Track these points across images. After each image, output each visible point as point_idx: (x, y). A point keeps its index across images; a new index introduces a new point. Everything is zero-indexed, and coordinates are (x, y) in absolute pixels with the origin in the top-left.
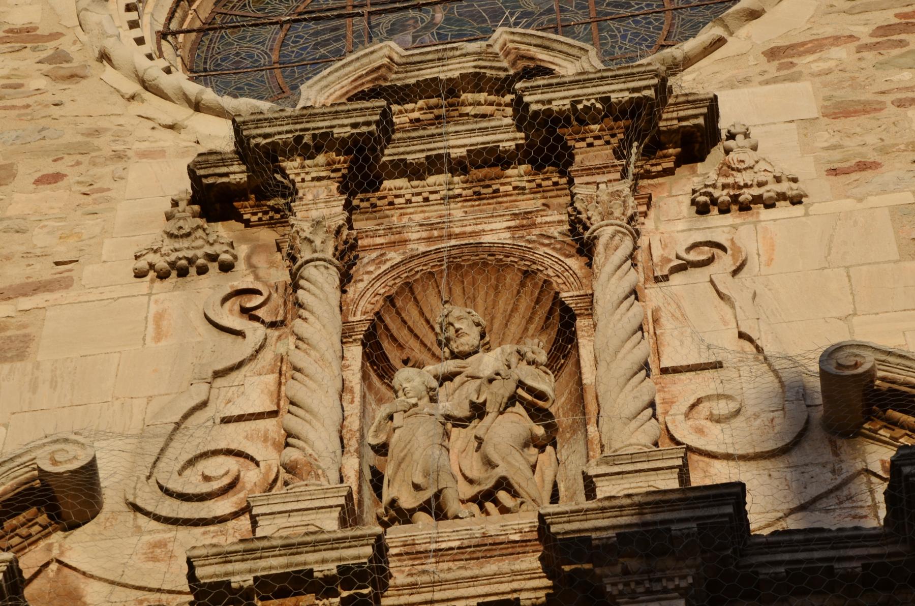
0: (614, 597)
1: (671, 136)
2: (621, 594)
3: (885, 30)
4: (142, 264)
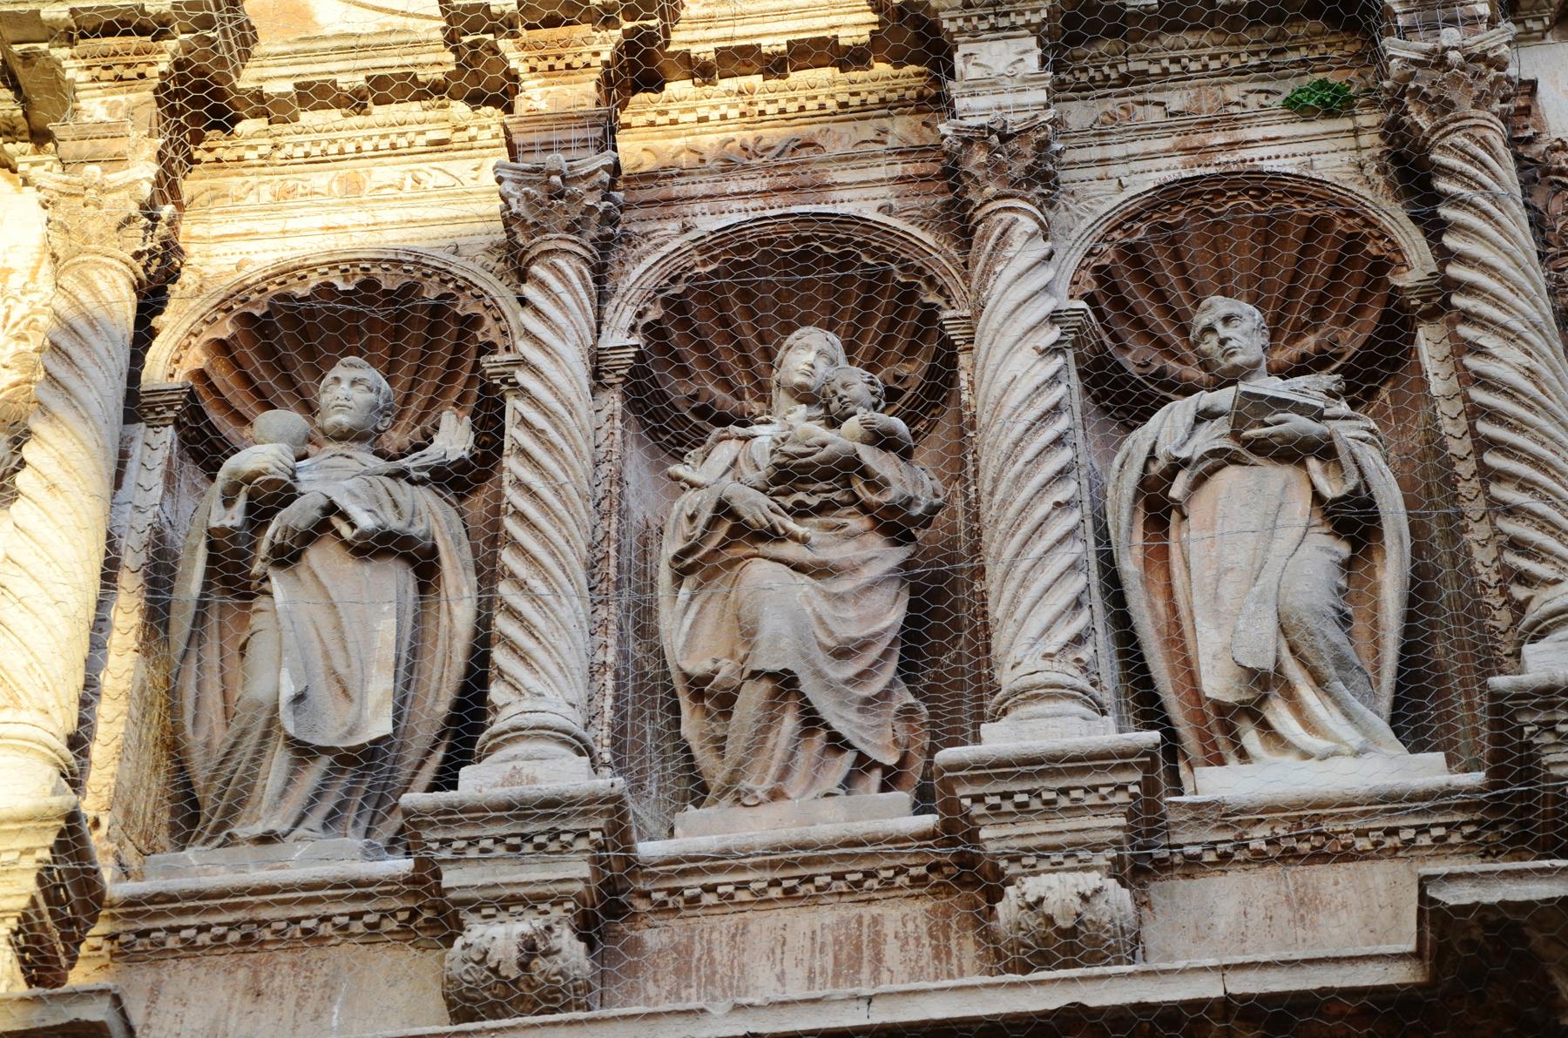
0: (951, 35)
2: (961, 31)
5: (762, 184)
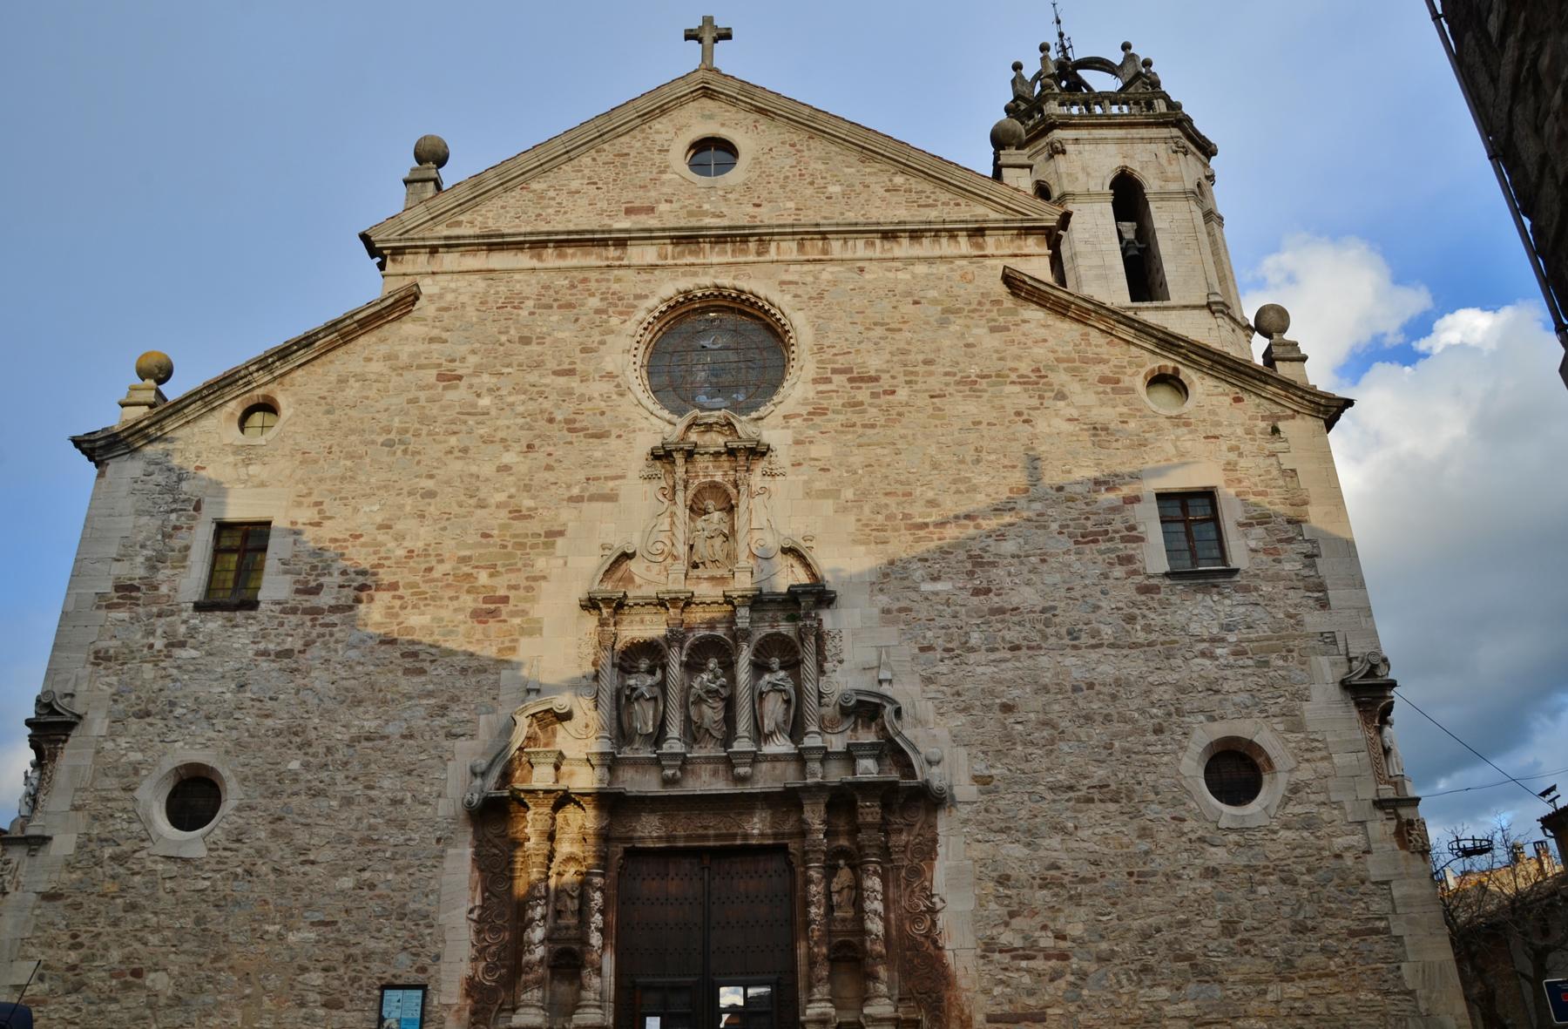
1: (758, 452)
3: (809, 413)
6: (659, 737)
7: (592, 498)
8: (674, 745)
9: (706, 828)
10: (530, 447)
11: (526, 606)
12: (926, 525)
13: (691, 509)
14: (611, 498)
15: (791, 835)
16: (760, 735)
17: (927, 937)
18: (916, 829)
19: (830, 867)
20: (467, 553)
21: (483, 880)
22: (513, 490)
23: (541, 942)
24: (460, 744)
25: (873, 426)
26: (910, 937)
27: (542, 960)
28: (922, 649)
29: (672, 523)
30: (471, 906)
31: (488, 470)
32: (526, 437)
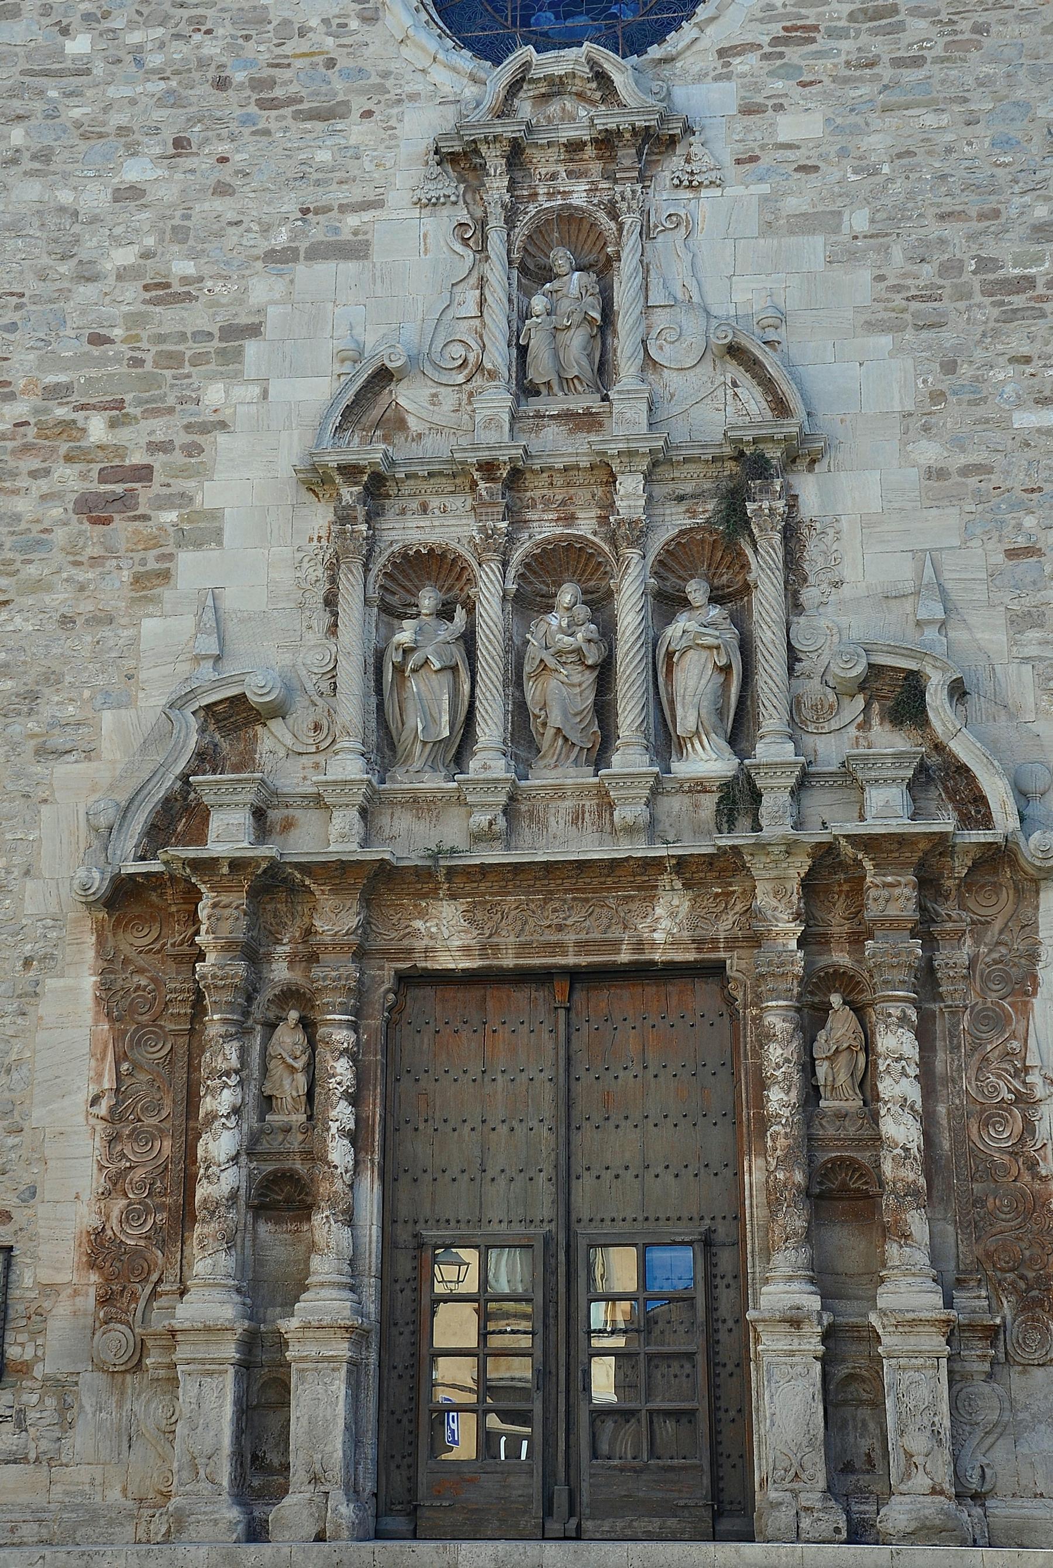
3: (776, 41)
4: (415, 199)
5: (555, 516)
6: (460, 747)
7: (317, 253)
8: (489, 761)
9: (560, 928)
10: (179, 143)
11: (181, 485)
12: (1030, 282)
13: (523, 269)
14: (355, 250)
15: (732, 944)
16: (665, 742)
17: (1014, 1154)
18: (992, 933)
19: (813, 1007)
20: (63, 378)
21: (118, 1037)
22: (150, 241)
23: (235, 1159)
24: (64, 770)
25: (917, 62)
26: (975, 1152)
27: (233, 1196)
28: (1012, 554)
29: (482, 302)
30: (94, 1090)
31: (95, 198)
32: (171, 122)
